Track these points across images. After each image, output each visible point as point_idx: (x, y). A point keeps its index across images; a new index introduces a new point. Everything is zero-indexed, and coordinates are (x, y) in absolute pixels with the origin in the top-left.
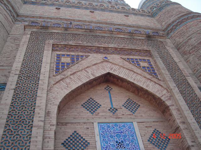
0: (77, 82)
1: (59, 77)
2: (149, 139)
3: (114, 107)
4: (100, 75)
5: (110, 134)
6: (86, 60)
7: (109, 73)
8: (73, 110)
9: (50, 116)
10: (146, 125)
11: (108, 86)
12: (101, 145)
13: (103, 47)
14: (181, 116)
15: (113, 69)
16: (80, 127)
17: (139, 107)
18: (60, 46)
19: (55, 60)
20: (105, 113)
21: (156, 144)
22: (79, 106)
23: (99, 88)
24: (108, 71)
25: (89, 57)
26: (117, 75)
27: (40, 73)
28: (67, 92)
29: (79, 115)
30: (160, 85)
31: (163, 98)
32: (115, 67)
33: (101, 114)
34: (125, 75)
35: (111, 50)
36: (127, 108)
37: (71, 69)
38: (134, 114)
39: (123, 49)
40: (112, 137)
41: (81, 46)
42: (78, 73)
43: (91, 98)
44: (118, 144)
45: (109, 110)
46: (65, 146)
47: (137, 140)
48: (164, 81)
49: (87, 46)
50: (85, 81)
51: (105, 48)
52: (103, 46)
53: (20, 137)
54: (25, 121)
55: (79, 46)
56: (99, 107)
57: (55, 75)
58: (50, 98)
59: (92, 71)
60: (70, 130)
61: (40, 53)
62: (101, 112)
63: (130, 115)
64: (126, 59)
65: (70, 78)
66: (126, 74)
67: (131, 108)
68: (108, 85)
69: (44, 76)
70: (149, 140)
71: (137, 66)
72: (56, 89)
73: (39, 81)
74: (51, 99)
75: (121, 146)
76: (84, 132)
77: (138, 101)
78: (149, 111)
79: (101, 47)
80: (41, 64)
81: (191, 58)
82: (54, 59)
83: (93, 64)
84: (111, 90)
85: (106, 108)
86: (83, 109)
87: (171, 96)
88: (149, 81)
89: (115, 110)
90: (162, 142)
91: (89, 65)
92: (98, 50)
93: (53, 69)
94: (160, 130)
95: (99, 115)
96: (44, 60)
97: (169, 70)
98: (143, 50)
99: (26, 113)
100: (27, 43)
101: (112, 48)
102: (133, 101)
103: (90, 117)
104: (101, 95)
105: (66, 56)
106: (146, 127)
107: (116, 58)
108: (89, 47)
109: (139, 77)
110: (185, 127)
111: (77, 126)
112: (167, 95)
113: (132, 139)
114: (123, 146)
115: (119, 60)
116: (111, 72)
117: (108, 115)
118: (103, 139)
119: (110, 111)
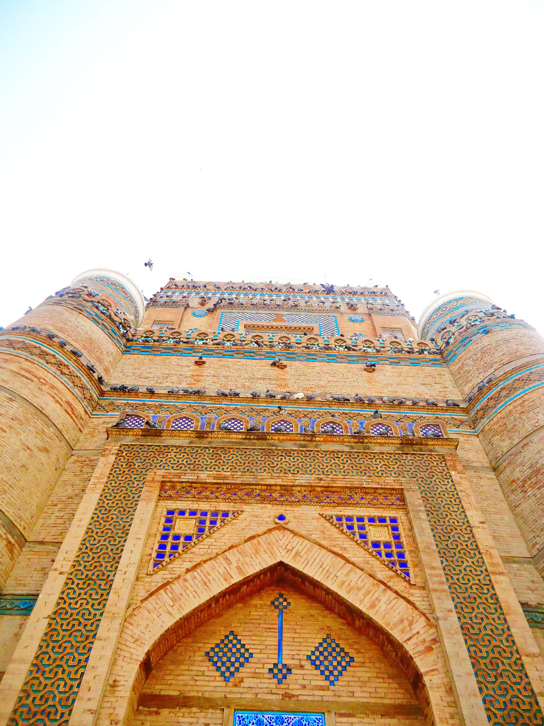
0: (199, 591)
3: (284, 662)
6: (233, 524)
7: (281, 564)
8: (183, 667)
9: (117, 694)
11: (281, 595)
13: (281, 486)
14: (452, 710)
15: (294, 551)
16: (191, 720)
17: (351, 664)
18: (178, 484)
20: (259, 680)
22: (199, 657)
23: (256, 601)
24: (278, 560)
25: (241, 517)
26: (300, 570)
27: (117, 567)
28: (169, 622)
29: (192, 683)
30: (409, 602)
31: (409, 647)
32: (299, 544)
33: (247, 682)
34: (321, 569)
35: (299, 492)
36: (317, 668)
37: (192, 553)
38: (332, 688)
39: (330, 489)
41: (227, 484)
42: (205, 565)
43: (232, 633)
45: (271, 670)
48: (424, 588)
49: (241, 484)
51: (284, 488)
52: (279, 482)
54: (53, 710)
55: (224, 484)
56: (247, 660)
57: (152, 572)
58: (126, 640)
59: (241, 559)
61: (128, 510)
62: (249, 675)
63: (322, 688)
64: (334, 518)
65: (185, 580)
66: (323, 567)
67: (327, 668)
68: (283, 592)
69: (124, 576)
71: (356, 542)
72: (145, 613)
74: (128, 643)
77: (351, 646)
78: (377, 677)
79: (276, 485)
80: (125, 541)
81: (526, 506)
82: (159, 523)
83: (248, 536)
84: (286, 607)
85: (264, 664)
87: (434, 641)
88: (382, 587)
89: (284, 671)
91: (235, 540)
92: (266, 494)
93: (150, 555)
95: (242, 685)
97: (443, 554)
98: (382, 489)
99: (61, 689)
100: (105, 480)
101: (301, 486)
102: (338, 645)
103: (219, 689)
104: (260, 622)
105: (187, 515)
107: (307, 517)
108: (247, 487)
109: (356, 576)
111: (183, 717)
112: (423, 637)
116: (287, 561)
117: (266, 685)
119: (271, 676)
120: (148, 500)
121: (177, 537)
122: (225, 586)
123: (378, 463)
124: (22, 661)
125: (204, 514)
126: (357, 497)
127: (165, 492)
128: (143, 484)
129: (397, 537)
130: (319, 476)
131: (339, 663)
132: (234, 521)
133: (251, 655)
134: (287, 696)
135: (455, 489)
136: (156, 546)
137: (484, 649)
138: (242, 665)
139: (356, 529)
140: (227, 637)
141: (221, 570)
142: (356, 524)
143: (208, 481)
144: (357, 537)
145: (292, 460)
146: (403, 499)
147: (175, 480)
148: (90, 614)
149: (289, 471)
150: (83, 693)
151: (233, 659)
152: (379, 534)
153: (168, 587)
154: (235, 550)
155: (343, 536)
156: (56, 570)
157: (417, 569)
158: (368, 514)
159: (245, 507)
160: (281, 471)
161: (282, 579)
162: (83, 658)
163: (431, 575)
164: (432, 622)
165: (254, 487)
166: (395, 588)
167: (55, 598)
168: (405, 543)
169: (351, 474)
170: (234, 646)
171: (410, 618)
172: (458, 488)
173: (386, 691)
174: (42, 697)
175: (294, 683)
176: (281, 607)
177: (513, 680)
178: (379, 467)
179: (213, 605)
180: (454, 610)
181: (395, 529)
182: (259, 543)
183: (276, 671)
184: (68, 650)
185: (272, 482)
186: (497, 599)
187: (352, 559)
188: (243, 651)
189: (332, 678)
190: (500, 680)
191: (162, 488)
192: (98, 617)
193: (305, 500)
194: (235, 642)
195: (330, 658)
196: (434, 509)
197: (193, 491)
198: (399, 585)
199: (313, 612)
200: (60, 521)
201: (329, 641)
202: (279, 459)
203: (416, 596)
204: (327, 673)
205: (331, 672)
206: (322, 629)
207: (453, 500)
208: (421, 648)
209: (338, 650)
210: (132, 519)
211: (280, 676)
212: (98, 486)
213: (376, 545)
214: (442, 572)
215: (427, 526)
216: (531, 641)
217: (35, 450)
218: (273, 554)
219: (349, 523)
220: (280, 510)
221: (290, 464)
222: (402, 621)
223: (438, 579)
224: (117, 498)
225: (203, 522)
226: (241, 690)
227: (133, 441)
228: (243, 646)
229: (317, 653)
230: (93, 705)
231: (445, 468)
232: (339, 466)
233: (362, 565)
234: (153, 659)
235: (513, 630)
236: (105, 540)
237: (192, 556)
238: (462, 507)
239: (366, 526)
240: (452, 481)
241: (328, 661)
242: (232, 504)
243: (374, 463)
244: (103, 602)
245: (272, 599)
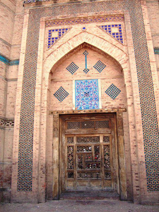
1: (50, 51)
2: (106, 91)
3: (87, 68)
7: (85, 43)
8: (61, 72)
10: (106, 81)
11: (86, 51)
13: (83, 17)
19: (48, 36)
21: (110, 94)
23: (79, 53)
25: (71, 30)
28: (55, 62)
29: (64, 75)
31: (120, 62)
32: (90, 36)
33: (78, 74)
35: (90, 19)
43: (73, 62)
45: (84, 71)
46: (55, 96)
52: (83, 16)
56: (77, 69)
60: (58, 86)
61: (37, 32)
63: (97, 74)
64: (101, 26)
65: (57, 51)
68: (86, 50)
69: (40, 52)
70: (106, 92)
72: (48, 61)
73: (37, 57)
75: (87, 95)
76: (66, 87)
77: (105, 63)
80: (38, 42)
83: (74, 35)
84: (87, 54)
88: (114, 46)
89: (87, 70)
90: (114, 93)
91: (71, 37)
92: (79, 21)
93: (46, 45)
94: (116, 84)
96: (40, 38)
100: (28, 23)
101: (90, 17)
102: (102, 63)
105: (55, 31)
107: (92, 27)
108: (72, 19)
109: (107, 44)
115: (95, 29)
116: (86, 42)
120: (42, 28)
121: (53, 39)
122: (69, 51)
124: (20, 76)
125: (60, 30)
127: (47, 24)
128: (40, 23)
129: (120, 31)
131: (102, 67)
132: (70, 31)
133: (78, 67)
136: (48, 42)
138: (76, 70)
139: (108, 29)
140: (71, 64)
141: (67, 47)
142: (108, 27)
143: (60, 19)
144: (108, 32)
147: (49, 20)
148: (34, 63)
149: (86, 11)
151: (74, 69)
153: (53, 53)
154: (71, 40)
155: (104, 32)
156: (21, 53)
159: (73, 26)
160: (83, 12)
161: (85, 46)
162: (35, 73)
165: (75, 19)
166: (118, 47)
167: (24, 60)
170: (74, 66)
171: (122, 55)
173: (114, 73)
174: (28, 83)
175: (90, 73)
176: (86, 54)
179: (66, 56)
181: (120, 28)
182: (78, 37)
183: (85, 71)
184: (31, 72)
185: (80, 16)
187: (106, 39)
188: (76, 67)
189: (100, 71)
191: (46, 23)
192: (36, 63)
194: (74, 65)
195: (100, 66)
197: (56, 23)
199: (95, 55)
201: (99, 62)
202: (82, 7)
203: (124, 49)
204: (99, 70)
205: (100, 70)
206: (98, 59)
208: (124, 62)
209: (102, 64)
210: (39, 35)
211: (86, 72)
212: (26, 26)
213: (114, 34)
219: (106, 28)
220: (84, 26)
221: (86, 9)
222: (119, 56)
224: (33, 29)
225: (60, 33)
226: (76, 76)
227: (33, 7)
228: (76, 65)
229: (96, 65)
233: (109, 41)
234: (53, 72)
237: (58, 43)
239: (111, 28)
242: (68, 26)
244: (36, 59)
245: (83, 52)
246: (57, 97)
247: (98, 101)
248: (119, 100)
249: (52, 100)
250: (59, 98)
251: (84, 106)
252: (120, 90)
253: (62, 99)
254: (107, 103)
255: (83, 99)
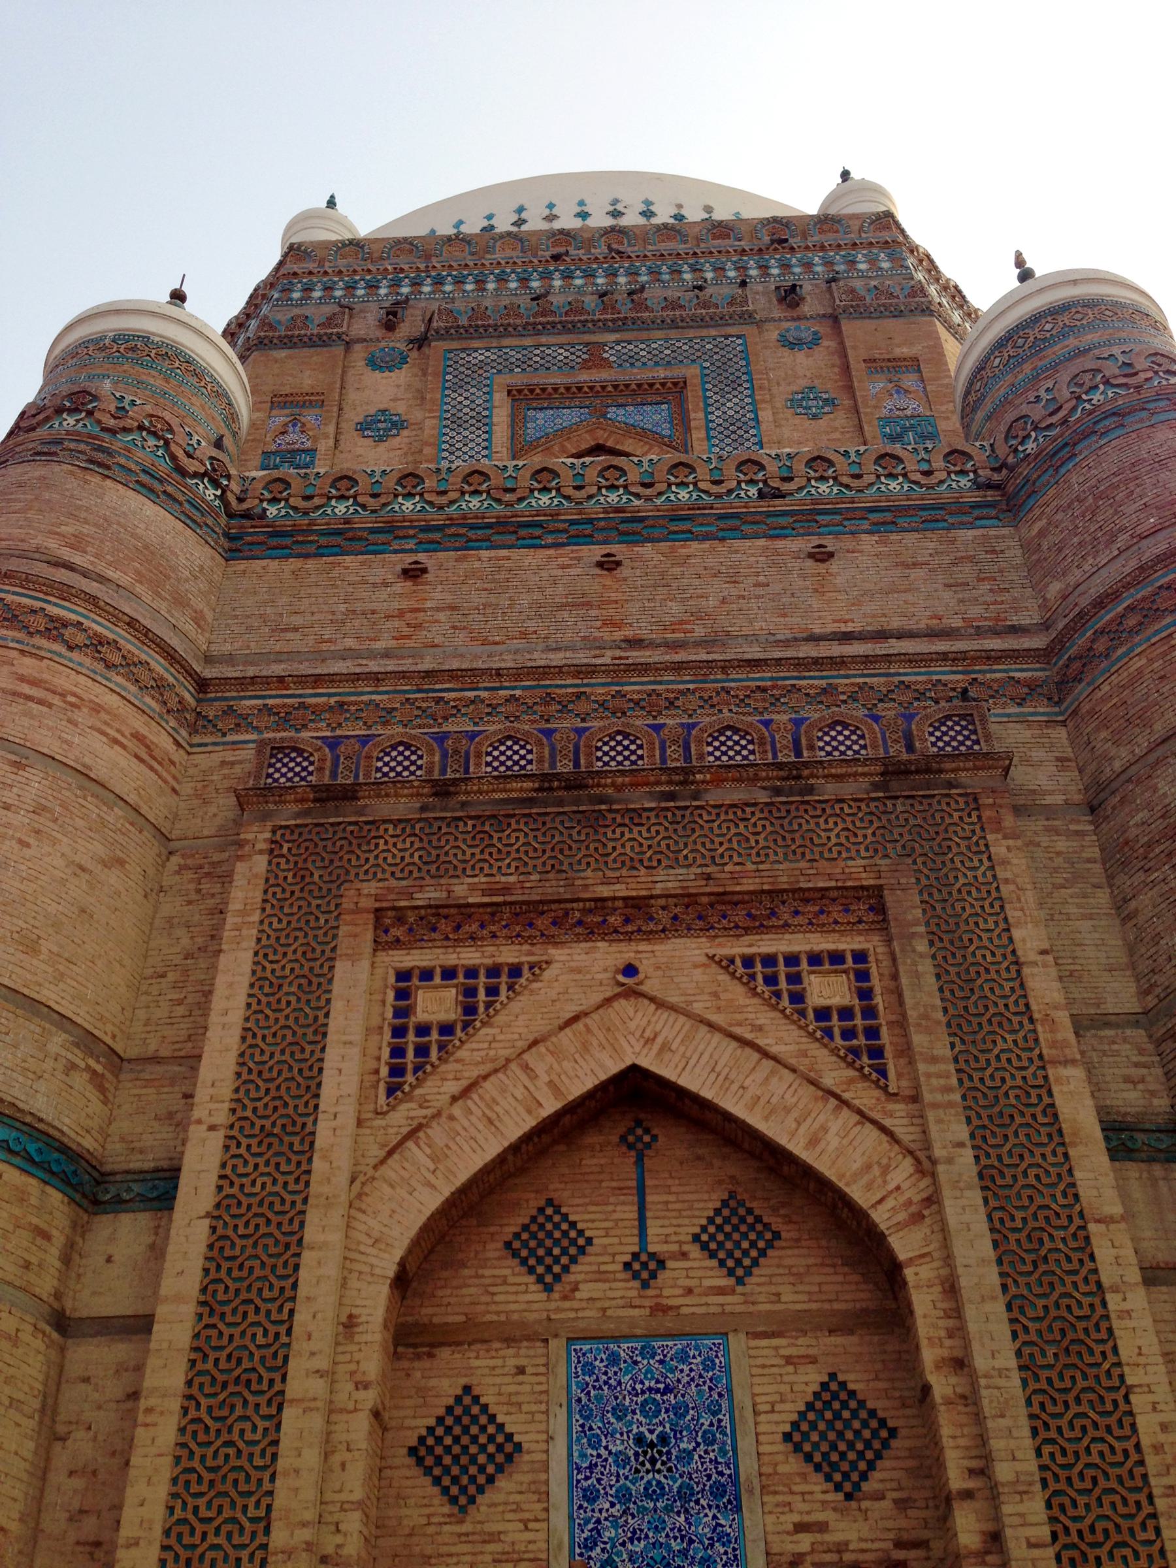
0: (479, 1137)
1: (402, 1116)
3: (652, 1248)
4: (589, 1083)
5: (616, 1398)
6: (532, 992)
8: (466, 1272)
9: (357, 1338)
11: (639, 1123)
12: (570, 1455)
13: (624, 899)
14: (950, 1323)
15: (659, 1040)
16: (492, 1363)
17: (776, 1243)
18: (410, 913)
19: (389, 1014)
20: (607, 1285)
21: (817, 1458)
22: (494, 1249)
24: (629, 1063)
25: (548, 974)
26: (673, 1078)
27: (316, 1107)
28: (431, 1202)
29: (487, 1299)
30: (883, 1129)
31: (881, 1217)
32: (669, 1027)
33: (585, 1291)
34: (713, 1075)
35: (663, 908)
36: (712, 1255)
37: (457, 1061)
38: (739, 1289)
39: (727, 898)
40: (620, 1412)
41: (511, 903)
42: (487, 1085)
43: (550, 1202)
44: (645, 1453)
46: (420, 1461)
47: (733, 1431)
49: (541, 902)
50: (517, 1125)
51: (630, 902)
52: (621, 890)
53: (239, 1451)
54: (254, 1376)
55: (505, 903)
57: (385, 1108)
58: (359, 1243)
59: (556, 1066)
60: (446, 1383)
61: (316, 986)
62: (588, 1277)
63: (721, 1291)
64: (738, 962)
65: (452, 1118)
66: (717, 1069)
67: (730, 1254)
68: (642, 1116)
69: (334, 1124)
70: (787, 1437)
71: (783, 1011)
72: (386, 1189)
73: (310, 1160)
74: (362, 1248)
75: (653, 1461)
76: (504, 1389)
77: (775, 1210)
78: (822, 1265)
79: (614, 899)
80: (323, 1049)
81: (1145, 901)
82: (384, 1002)
85: (614, 1255)
86: (509, 1269)
87: (929, 1201)
88: (833, 1102)
89: (652, 1265)
91: (541, 1025)
92: (594, 920)
93: (377, 1072)
94: (856, 1380)
95: (578, 1295)
97: (954, 1028)
98: (838, 888)
99: (260, 1340)
100: (256, 917)
102: (750, 1211)
103: (535, 1306)
104: (601, 1177)
105: (438, 980)
106: (789, 1360)
107: (683, 963)
108: (553, 907)
109: (782, 1086)
110: (959, 1390)
111: (477, 1358)
112: (908, 1195)
113: (711, 1424)
114: (663, 1463)
115: (698, 975)
116: (644, 1063)
117: (619, 1294)
118: (582, 1426)
119: (629, 1275)
120: (354, 958)
121: (423, 1030)
122: (530, 1123)
123: (831, 825)
124: (179, 1299)
125: (471, 973)
126: (785, 913)
128: (337, 918)
130: (705, 870)
131: (753, 1244)
132: (535, 985)
133: (589, 1241)
134: (660, 1309)
135: (994, 876)
136: (386, 1053)
137: (1019, 1215)
138: (574, 1260)
140: (541, 1210)
141: (519, 1093)
143: (471, 900)
144: (785, 1002)
145: (645, 834)
146: (880, 909)
147: (403, 904)
148: (283, 1201)
149: (641, 861)
150: (299, 1345)
151: (556, 1251)
152: (828, 990)
153: (421, 1134)
154: (542, 1048)
155: (755, 1001)
156: (199, 1122)
157: (902, 1061)
158: (807, 948)
159: (555, 953)
160: (623, 862)
162: (288, 1284)
163: (929, 1075)
164: (925, 1165)
165: (569, 906)
166: (857, 1102)
167: (212, 1179)
168: (881, 1008)
169: (772, 857)
170: (557, 1226)
172: (1001, 874)
173: (839, 1288)
174: (229, 1356)
175: (672, 1283)
176: (640, 1146)
177: (1067, 1266)
178: (833, 835)
179: (510, 1158)
180: (968, 1143)
182: (588, 1030)
183: (636, 1266)
184: (258, 1272)
185: (605, 891)
186: (1056, 1115)
187: (774, 1050)
188: (573, 1234)
189: (740, 1272)
190: (1043, 1267)
191: (378, 925)
192: (299, 1206)
193: (676, 927)
194: (557, 1218)
195: (736, 1236)
196: (944, 927)
197: (442, 925)
198: (865, 1096)
199: (700, 1152)
200: (180, 1010)
201: (732, 1203)
202: (618, 835)
204: (730, 1263)
205: (738, 1262)
206: (720, 1182)
207: (987, 904)
209: (750, 1219)
210: (328, 1001)
211: (645, 1275)
212: (244, 932)
213: (823, 1014)
214: (952, 1068)
215: (926, 967)
216: (1110, 1194)
217: (97, 869)
218: (616, 1051)
219: (769, 970)
220: (626, 952)
221: (641, 845)
223: (942, 1082)
224: (290, 956)
225: (471, 992)
226: (575, 1304)
227: (298, 815)
228: (573, 1225)
229: (712, 1229)
230: (322, 1363)
231: (977, 827)
232: (748, 840)
233: (793, 1061)
234: (411, 1268)
235: (1078, 1174)
236: (283, 1052)
237: (459, 1066)
238: (1006, 919)
240: (989, 858)
241: (734, 1242)
242: (526, 947)
243: (823, 826)
246: (437, 1471)
247: (738, 1509)
248: (886, 1504)
249: (398, 1496)
250: (446, 1481)
251: (638, 1547)
252: (891, 1424)
253: (472, 1490)
254: (800, 1528)
255: (624, 1496)
